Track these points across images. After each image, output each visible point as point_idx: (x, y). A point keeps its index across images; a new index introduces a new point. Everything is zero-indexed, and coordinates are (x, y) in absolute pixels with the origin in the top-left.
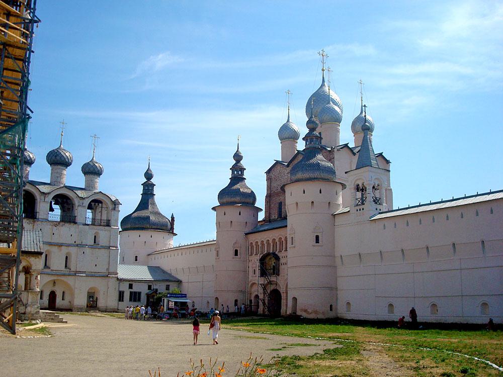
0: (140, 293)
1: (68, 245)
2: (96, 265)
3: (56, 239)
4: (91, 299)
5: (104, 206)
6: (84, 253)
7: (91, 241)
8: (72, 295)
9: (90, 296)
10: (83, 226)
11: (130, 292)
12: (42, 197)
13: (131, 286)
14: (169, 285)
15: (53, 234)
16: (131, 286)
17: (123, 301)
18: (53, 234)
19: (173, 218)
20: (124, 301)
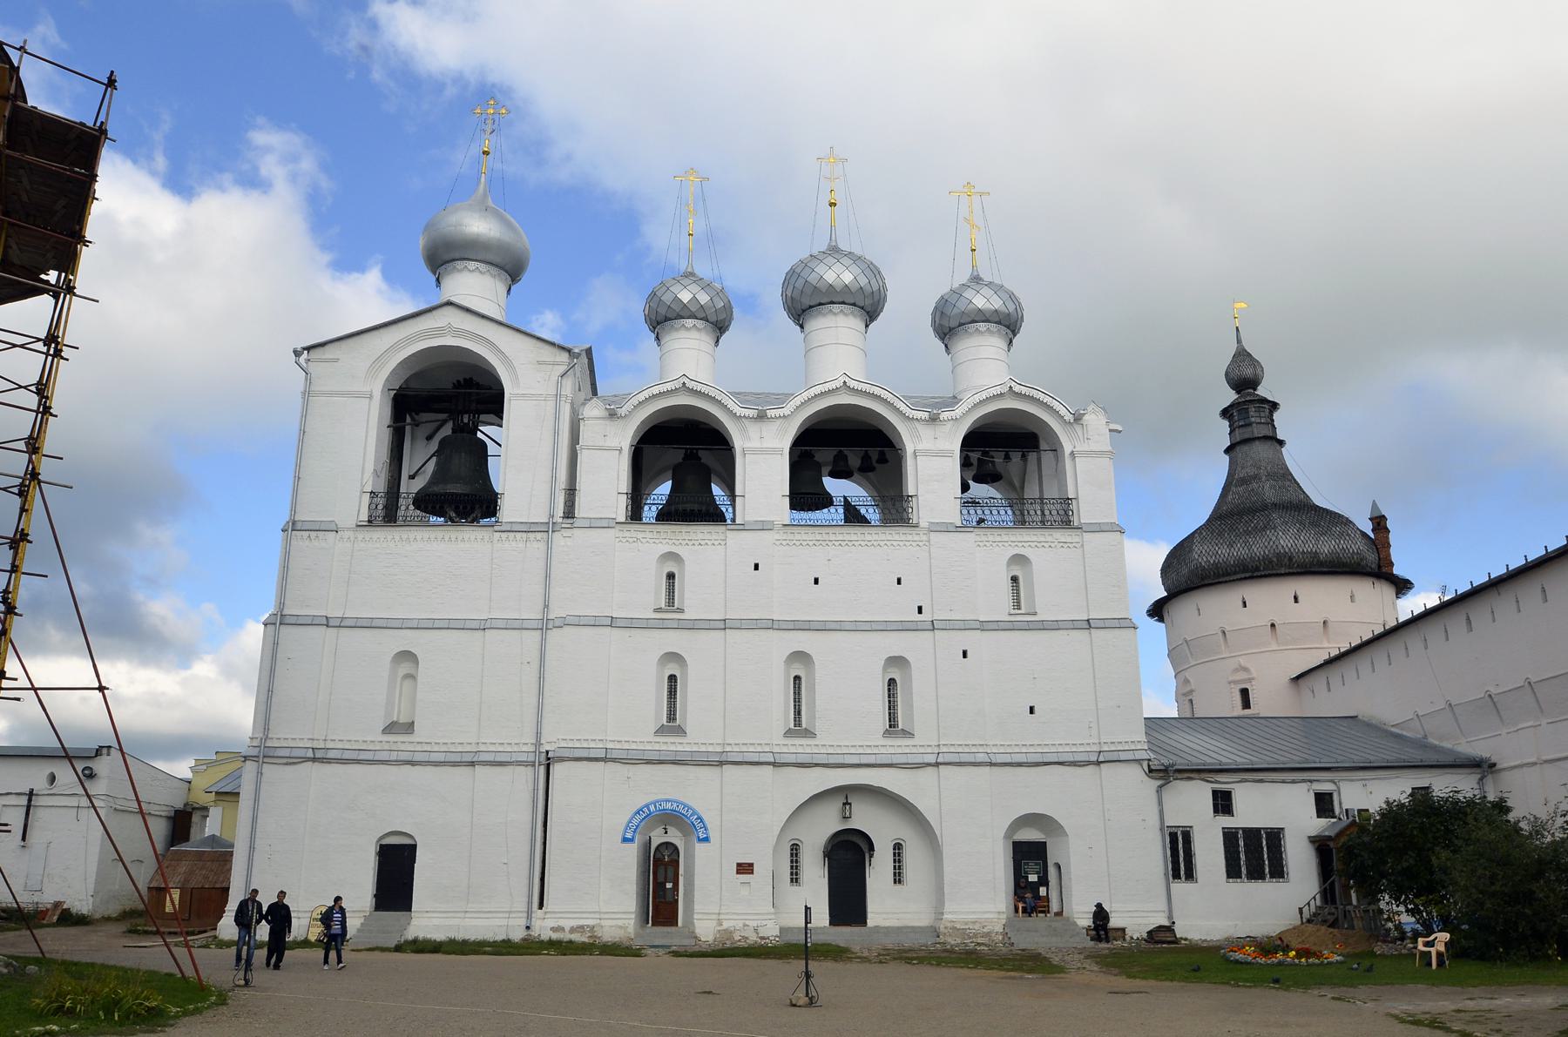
0: (1275, 836)
5: (1043, 445)
11: (1230, 837)
13: (1223, 803)
16: (1223, 803)
17: (1190, 876)
19: (1379, 522)
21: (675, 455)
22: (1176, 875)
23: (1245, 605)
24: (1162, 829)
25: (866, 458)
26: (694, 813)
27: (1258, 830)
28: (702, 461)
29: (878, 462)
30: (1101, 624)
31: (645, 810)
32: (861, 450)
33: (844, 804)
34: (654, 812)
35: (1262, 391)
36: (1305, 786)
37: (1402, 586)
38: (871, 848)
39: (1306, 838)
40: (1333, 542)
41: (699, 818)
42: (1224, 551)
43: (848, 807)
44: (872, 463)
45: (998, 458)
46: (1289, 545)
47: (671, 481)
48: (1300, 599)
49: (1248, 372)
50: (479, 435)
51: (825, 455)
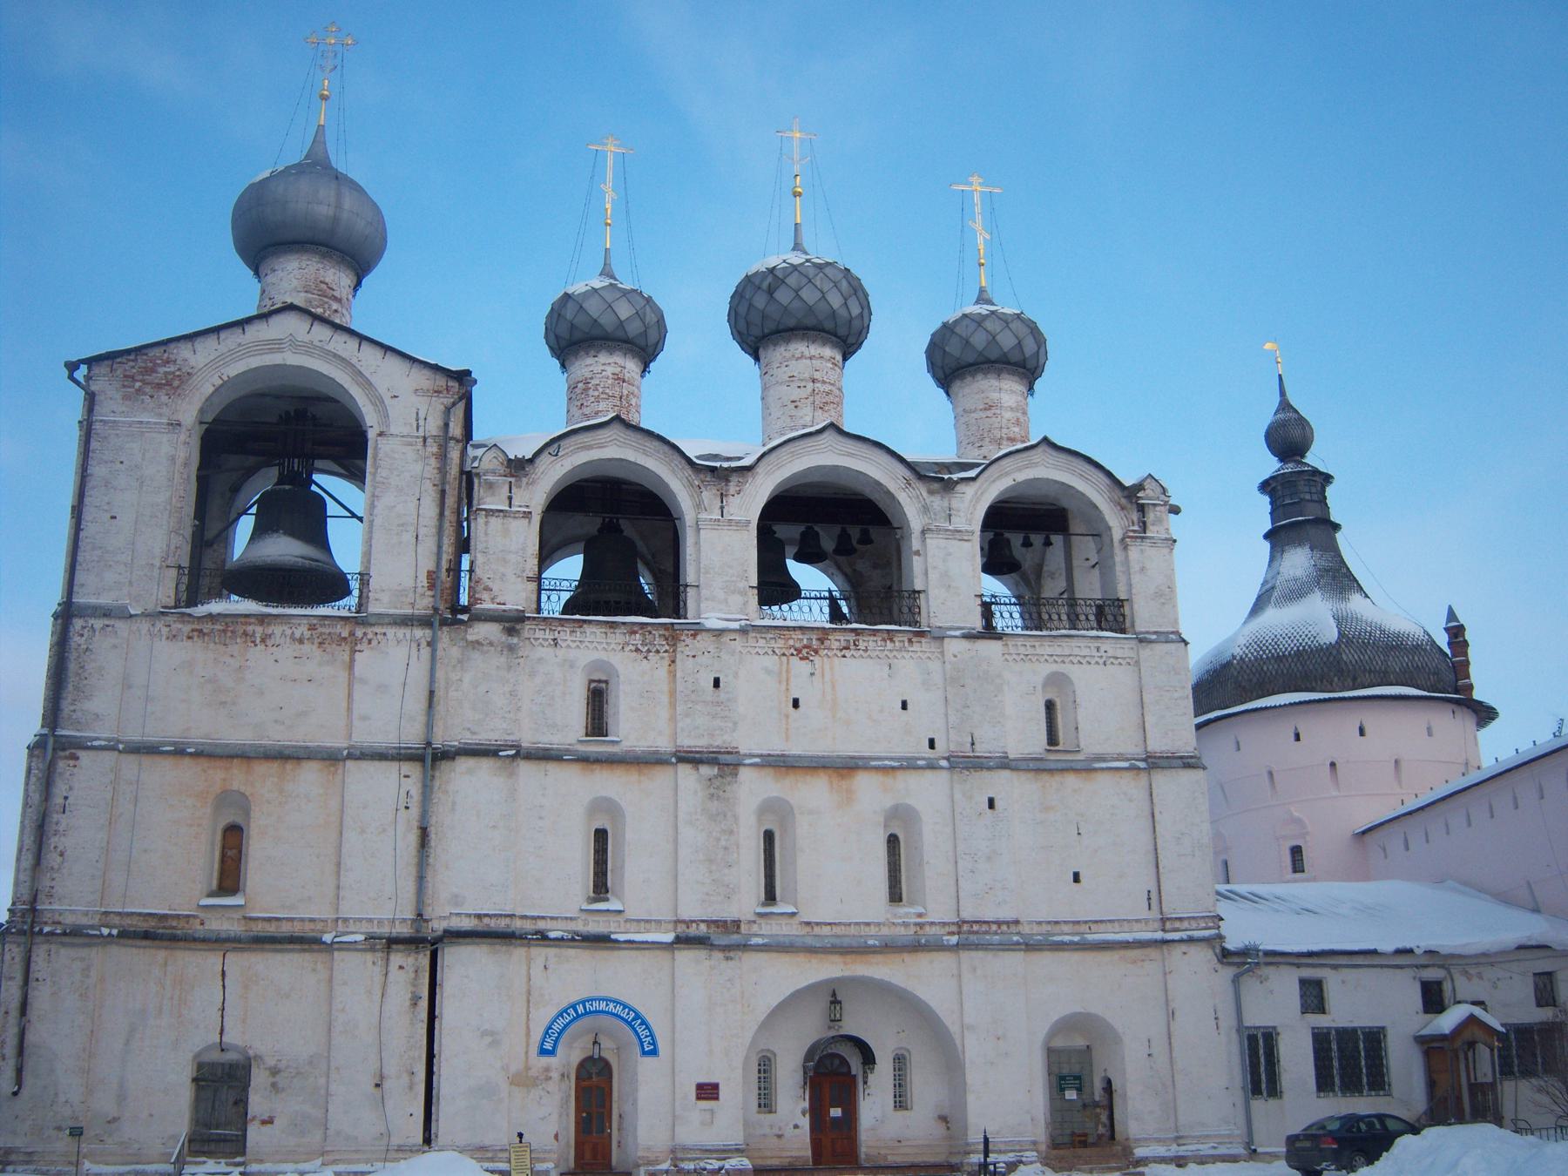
0: (1375, 1038)
2: (1076, 878)
4: (1071, 1095)
6: (991, 804)
7: (1035, 742)
8: (951, 1063)
9: (1062, 1078)
10: (965, 644)
11: (1321, 1040)
12: (709, 496)
13: (1313, 997)
14: (1549, 974)
15: (796, 704)
17: (1274, 1091)
18: (796, 704)
19: (1456, 633)
20: (1285, 1096)
21: (589, 524)
22: (1256, 1090)
23: (1297, 738)
24: (1238, 1031)
26: (638, 1016)
27: (1354, 1030)
28: (625, 534)
29: (860, 542)
31: (571, 1011)
32: (837, 529)
33: (832, 1003)
34: (582, 1015)
35: (1313, 458)
36: (1409, 973)
37: (1485, 714)
38: (868, 1058)
39: (1412, 1039)
40: (1406, 659)
41: (644, 1023)
42: (1271, 667)
43: (838, 1008)
44: (852, 544)
45: (1016, 539)
46: (1354, 662)
47: (582, 556)
48: (1367, 730)
49: (1296, 433)
51: (787, 531)
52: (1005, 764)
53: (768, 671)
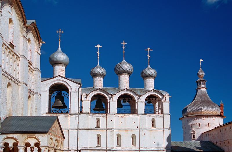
1: (131, 130)
3: (122, 127)
25: (129, 99)
30: (166, 129)
50: (62, 95)
52: (146, 129)
53: (118, 119)
